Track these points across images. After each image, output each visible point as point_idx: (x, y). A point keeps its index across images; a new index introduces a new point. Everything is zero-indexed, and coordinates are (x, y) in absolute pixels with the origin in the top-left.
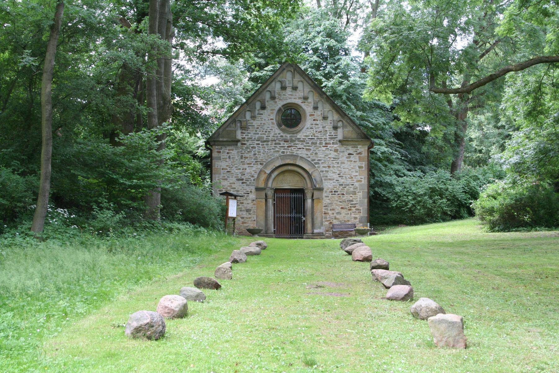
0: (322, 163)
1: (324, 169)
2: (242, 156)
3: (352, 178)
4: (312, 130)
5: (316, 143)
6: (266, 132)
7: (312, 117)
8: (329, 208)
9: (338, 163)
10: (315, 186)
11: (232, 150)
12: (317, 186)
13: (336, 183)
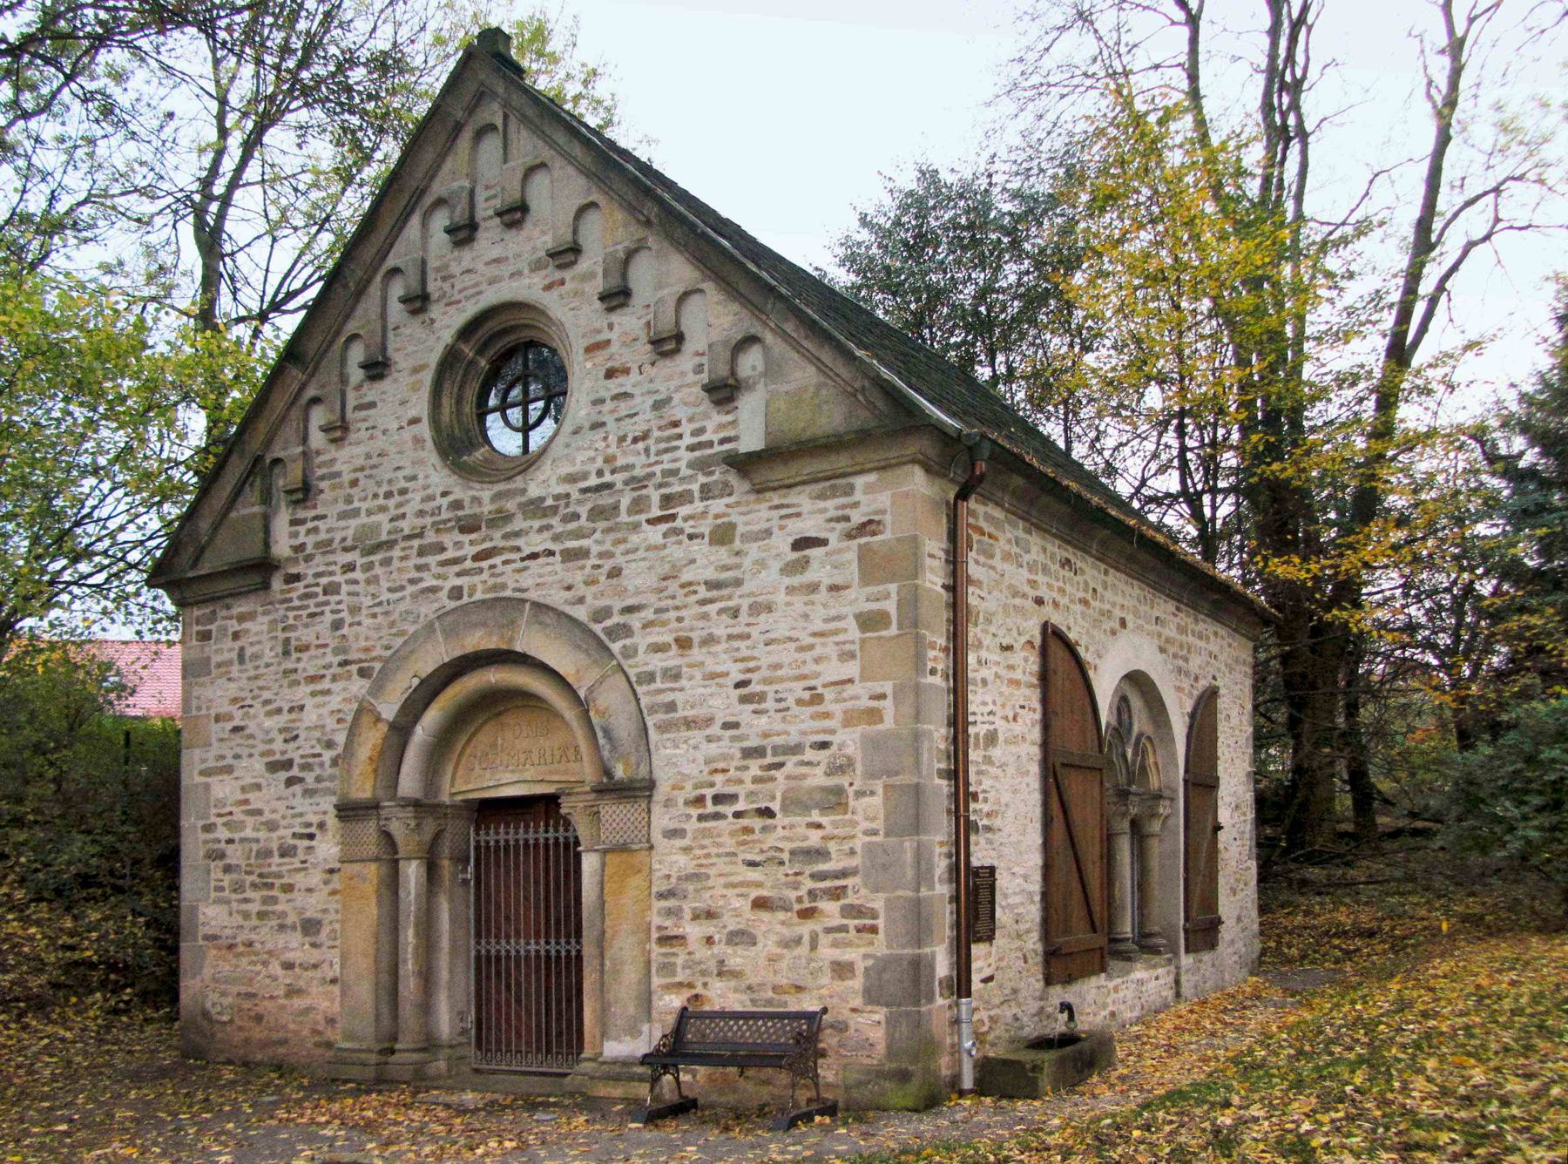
1: (657, 662)
2: (287, 641)
4: (601, 433)
5: (616, 507)
6: (389, 495)
7: (600, 357)
9: (735, 613)
11: (251, 616)
12: (620, 772)
13: (727, 746)
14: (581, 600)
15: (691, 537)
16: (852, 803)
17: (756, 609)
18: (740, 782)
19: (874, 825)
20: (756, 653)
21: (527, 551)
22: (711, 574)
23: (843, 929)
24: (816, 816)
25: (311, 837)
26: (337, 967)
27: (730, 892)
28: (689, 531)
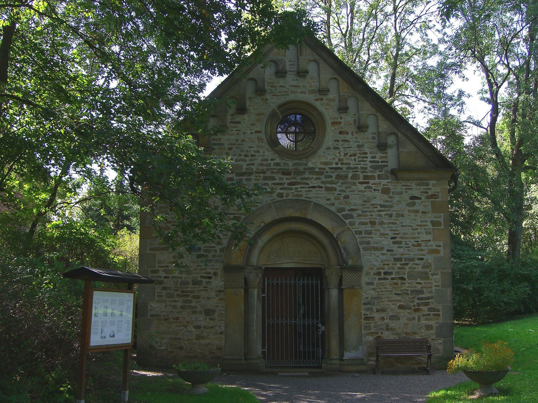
0: (359, 216)
1: (363, 228)
3: (420, 245)
5: (347, 176)
6: (246, 156)
7: (337, 126)
8: (374, 308)
9: (391, 216)
10: (345, 262)
12: (350, 262)
14: (333, 204)
15: (375, 190)
16: (431, 277)
17: (398, 215)
18: (394, 268)
19: (438, 284)
20: (398, 229)
21: (311, 185)
22: (381, 202)
23: (429, 315)
24: (419, 281)
25: (210, 278)
26: (223, 328)
27: (390, 303)
28: (374, 188)
